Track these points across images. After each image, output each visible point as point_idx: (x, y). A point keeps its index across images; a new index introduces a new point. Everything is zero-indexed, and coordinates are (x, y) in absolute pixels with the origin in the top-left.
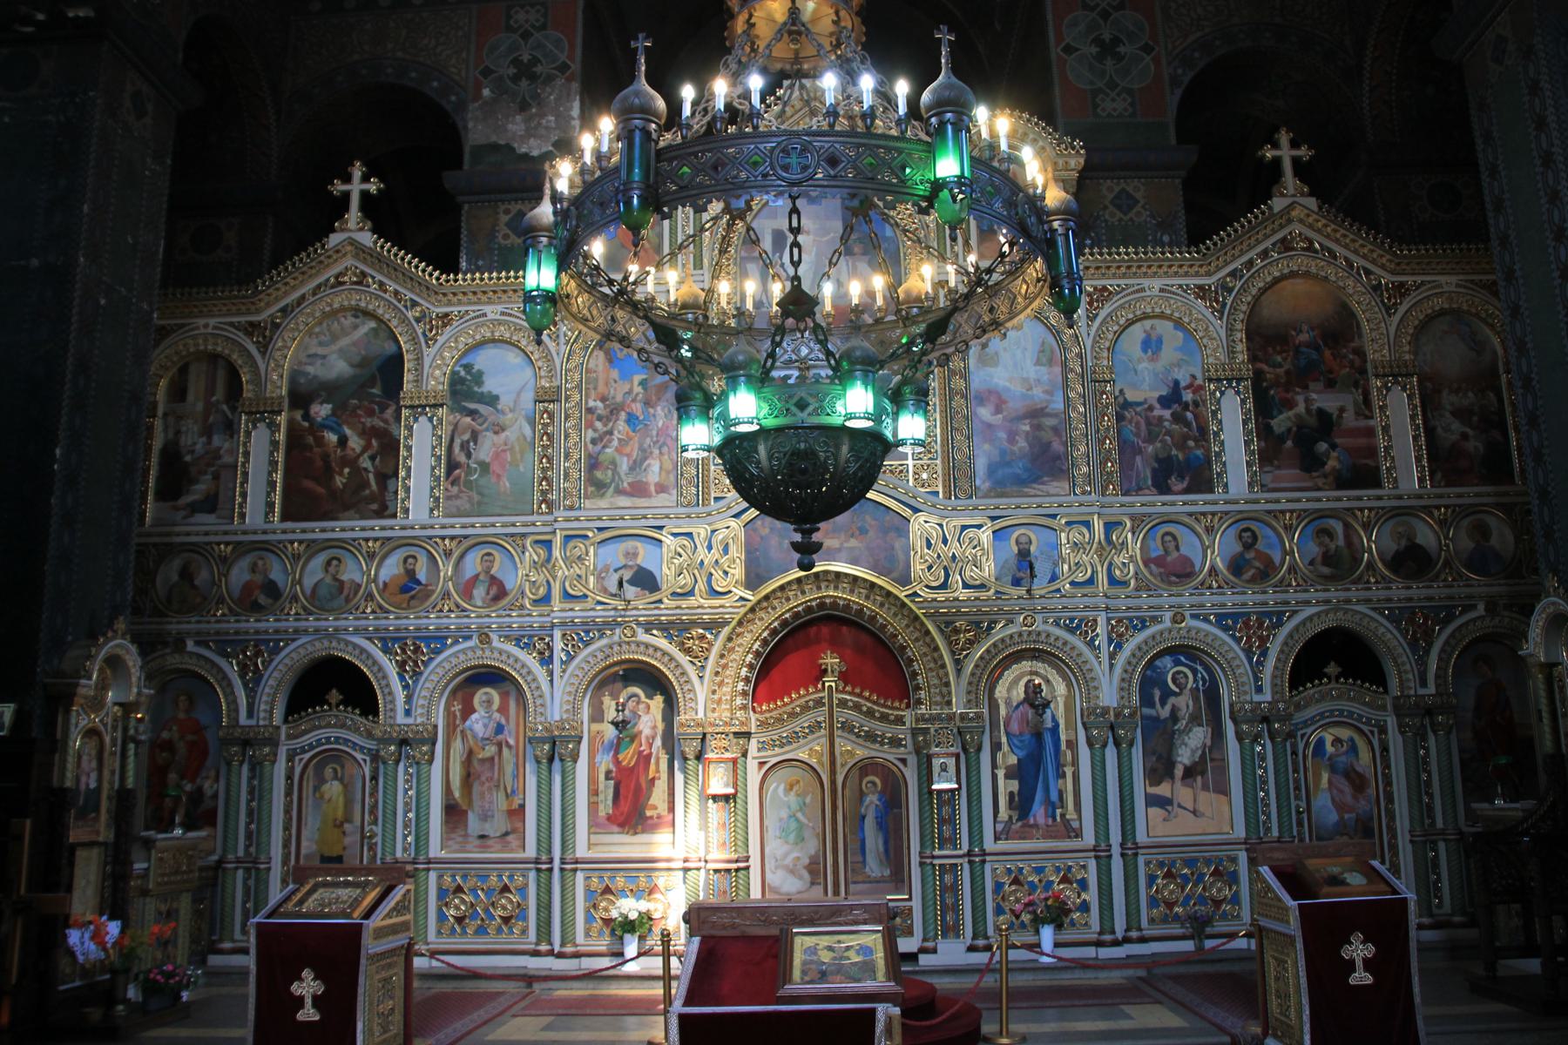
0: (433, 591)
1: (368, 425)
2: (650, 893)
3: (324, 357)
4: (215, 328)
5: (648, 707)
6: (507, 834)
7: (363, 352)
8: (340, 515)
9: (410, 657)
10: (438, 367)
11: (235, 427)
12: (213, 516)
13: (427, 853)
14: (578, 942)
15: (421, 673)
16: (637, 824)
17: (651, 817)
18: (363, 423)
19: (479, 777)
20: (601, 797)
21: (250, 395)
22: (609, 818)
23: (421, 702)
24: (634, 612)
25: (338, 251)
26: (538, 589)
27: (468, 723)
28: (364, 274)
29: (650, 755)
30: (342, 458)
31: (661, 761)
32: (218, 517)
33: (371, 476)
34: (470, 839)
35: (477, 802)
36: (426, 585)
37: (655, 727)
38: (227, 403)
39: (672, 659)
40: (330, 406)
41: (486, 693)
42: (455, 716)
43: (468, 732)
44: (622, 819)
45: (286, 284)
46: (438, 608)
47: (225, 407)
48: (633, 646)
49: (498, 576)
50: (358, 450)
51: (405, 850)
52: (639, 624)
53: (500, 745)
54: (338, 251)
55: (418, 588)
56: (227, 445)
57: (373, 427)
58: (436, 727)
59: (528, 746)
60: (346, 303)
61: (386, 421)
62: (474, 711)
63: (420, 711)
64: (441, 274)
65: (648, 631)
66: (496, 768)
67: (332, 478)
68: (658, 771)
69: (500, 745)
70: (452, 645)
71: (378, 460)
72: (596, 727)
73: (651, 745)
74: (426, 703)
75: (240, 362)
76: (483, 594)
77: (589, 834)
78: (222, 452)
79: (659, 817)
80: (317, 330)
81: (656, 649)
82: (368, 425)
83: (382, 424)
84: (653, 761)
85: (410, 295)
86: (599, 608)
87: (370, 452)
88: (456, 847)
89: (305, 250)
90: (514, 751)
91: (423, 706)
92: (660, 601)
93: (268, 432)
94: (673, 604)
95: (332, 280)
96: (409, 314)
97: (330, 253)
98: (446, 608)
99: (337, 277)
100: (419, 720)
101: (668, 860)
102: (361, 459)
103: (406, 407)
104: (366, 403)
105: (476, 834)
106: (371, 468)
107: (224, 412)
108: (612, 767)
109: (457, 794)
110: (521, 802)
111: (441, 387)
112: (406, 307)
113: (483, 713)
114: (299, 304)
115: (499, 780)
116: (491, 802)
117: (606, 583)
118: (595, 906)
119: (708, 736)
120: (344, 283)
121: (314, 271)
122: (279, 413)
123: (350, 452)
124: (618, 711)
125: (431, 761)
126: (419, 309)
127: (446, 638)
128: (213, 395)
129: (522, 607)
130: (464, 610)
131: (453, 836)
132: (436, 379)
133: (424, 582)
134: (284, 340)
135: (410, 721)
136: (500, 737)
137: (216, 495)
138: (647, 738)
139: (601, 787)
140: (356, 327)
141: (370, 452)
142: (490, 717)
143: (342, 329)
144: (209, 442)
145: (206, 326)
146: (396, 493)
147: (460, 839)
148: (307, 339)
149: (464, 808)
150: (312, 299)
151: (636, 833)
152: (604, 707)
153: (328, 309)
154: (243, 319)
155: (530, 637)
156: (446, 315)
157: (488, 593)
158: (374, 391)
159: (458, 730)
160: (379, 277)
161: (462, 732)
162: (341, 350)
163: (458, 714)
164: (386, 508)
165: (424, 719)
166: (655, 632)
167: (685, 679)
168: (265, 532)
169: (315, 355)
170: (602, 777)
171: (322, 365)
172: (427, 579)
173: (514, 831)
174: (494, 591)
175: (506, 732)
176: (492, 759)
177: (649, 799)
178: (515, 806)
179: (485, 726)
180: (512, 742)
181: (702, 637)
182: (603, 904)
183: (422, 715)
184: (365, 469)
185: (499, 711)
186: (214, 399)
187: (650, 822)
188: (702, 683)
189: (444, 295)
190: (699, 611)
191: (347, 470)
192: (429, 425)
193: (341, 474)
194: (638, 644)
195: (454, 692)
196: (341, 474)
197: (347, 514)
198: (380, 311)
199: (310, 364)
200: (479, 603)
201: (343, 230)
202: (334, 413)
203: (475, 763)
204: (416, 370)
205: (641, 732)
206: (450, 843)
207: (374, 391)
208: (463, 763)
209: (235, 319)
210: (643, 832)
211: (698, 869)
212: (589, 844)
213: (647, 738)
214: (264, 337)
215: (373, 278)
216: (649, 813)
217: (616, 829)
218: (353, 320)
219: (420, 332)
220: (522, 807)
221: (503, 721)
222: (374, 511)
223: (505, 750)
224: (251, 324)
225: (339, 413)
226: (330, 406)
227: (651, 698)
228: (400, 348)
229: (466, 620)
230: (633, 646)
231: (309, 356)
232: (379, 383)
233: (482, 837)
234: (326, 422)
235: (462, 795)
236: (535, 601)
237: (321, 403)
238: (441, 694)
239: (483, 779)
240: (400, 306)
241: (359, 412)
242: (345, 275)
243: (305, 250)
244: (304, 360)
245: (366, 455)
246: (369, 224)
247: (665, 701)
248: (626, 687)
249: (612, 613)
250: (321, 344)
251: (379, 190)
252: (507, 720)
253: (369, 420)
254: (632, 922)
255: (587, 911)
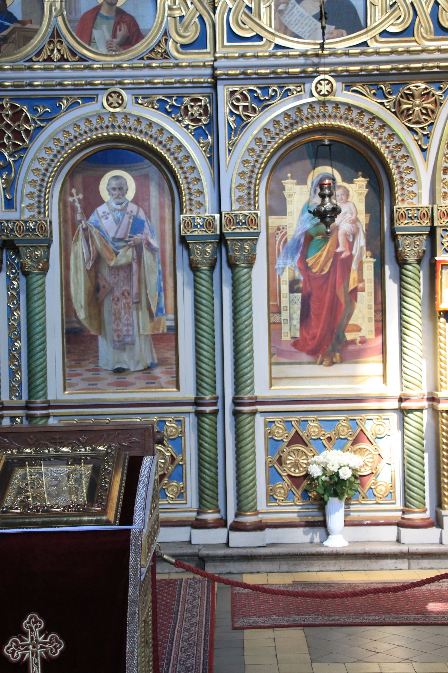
0: (36, 31)
2: (355, 442)
5: (347, 193)
6: (149, 368)
9: (8, 126)
13: (45, 394)
14: (259, 508)
15: (25, 149)
16: (334, 351)
17: (353, 342)
19: (112, 291)
20: (285, 315)
22: (296, 343)
23: (28, 189)
24: (332, 59)
26: (186, 29)
27: (92, 218)
29: (351, 257)
31: (365, 266)
34: (103, 375)
35: (109, 327)
36: (23, 23)
37: (356, 221)
39: (384, 125)
41: (116, 177)
42: (74, 209)
43: (94, 231)
44: (312, 344)
46: (44, 55)
48: (330, 108)
49: (129, 10)
51: (12, 390)
52: (338, 76)
53: (138, 248)
55: (12, 26)
58: (51, 222)
59: (179, 249)
62: (102, 202)
63: (27, 201)
65: (348, 87)
66: (135, 279)
68: (361, 280)
69: (138, 248)
70: (68, 108)
72: (274, 221)
73: (351, 246)
74: (35, 190)
76: (108, 36)
77: (271, 364)
79: (363, 341)
81: (362, 111)
84: (354, 266)
86: (279, 53)
88: (84, 385)
90: (158, 255)
91: (31, 195)
92: (365, 44)
94: (385, 47)
98: (56, 56)
100: (27, 215)
101: (380, 399)
105: (110, 368)
108: (298, 274)
109: (82, 315)
110: (172, 324)
113: (114, 205)
115: (139, 294)
116: (131, 325)
117: (286, 20)
118: (280, 461)
119: (439, 231)
124: (323, 196)
125: (44, 271)
127: (60, 99)
129: (166, 55)
130: (83, 59)
131: (79, 371)
133: (19, 17)
135: (13, 215)
136: (138, 237)
138: (346, 235)
139: (285, 302)
142: (123, 210)
147: (89, 375)
149: (93, 332)
151: (332, 363)
152: (286, 193)
155: (180, 98)
157: (114, 36)
159: (80, 227)
161: (85, 230)
163: (78, 205)
165: (35, 213)
166: (358, 88)
167: (403, 152)
170: (285, 288)
172: (24, 13)
173: (162, 362)
174: (120, 34)
175: (147, 230)
176: (129, 265)
177: (349, 318)
178: (163, 329)
179: (118, 222)
180: (155, 243)
181: (427, 95)
182: (291, 459)
183: (30, 207)
185: (135, 201)
187: (351, 348)
188: (426, 159)
190: (424, 56)
194: (337, 105)
195: (71, 174)
200: (103, 50)
203: (105, 272)
205: (337, 228)
206: (74, 380)
208: (88, 272)
210: (342, 361)
211: (421, 410)
212: (271, 378)
213: (346, 235)
216: (349, 336)
217: (305, 357)
220: (174, 330)
221: (142, 215)
223: (146, 255)
227: (351, 181)
229: (87, 73)
230: (330, 108)
233: (119, 371)
235: (89, 316)
236: (183, 46)
238: (56, 177)
239: (117, 293)
247: (369, 185)
248: (314, 168)
249: (301, 60)
252: (148, 214)
254: (341, 482)
255: (270, 467)
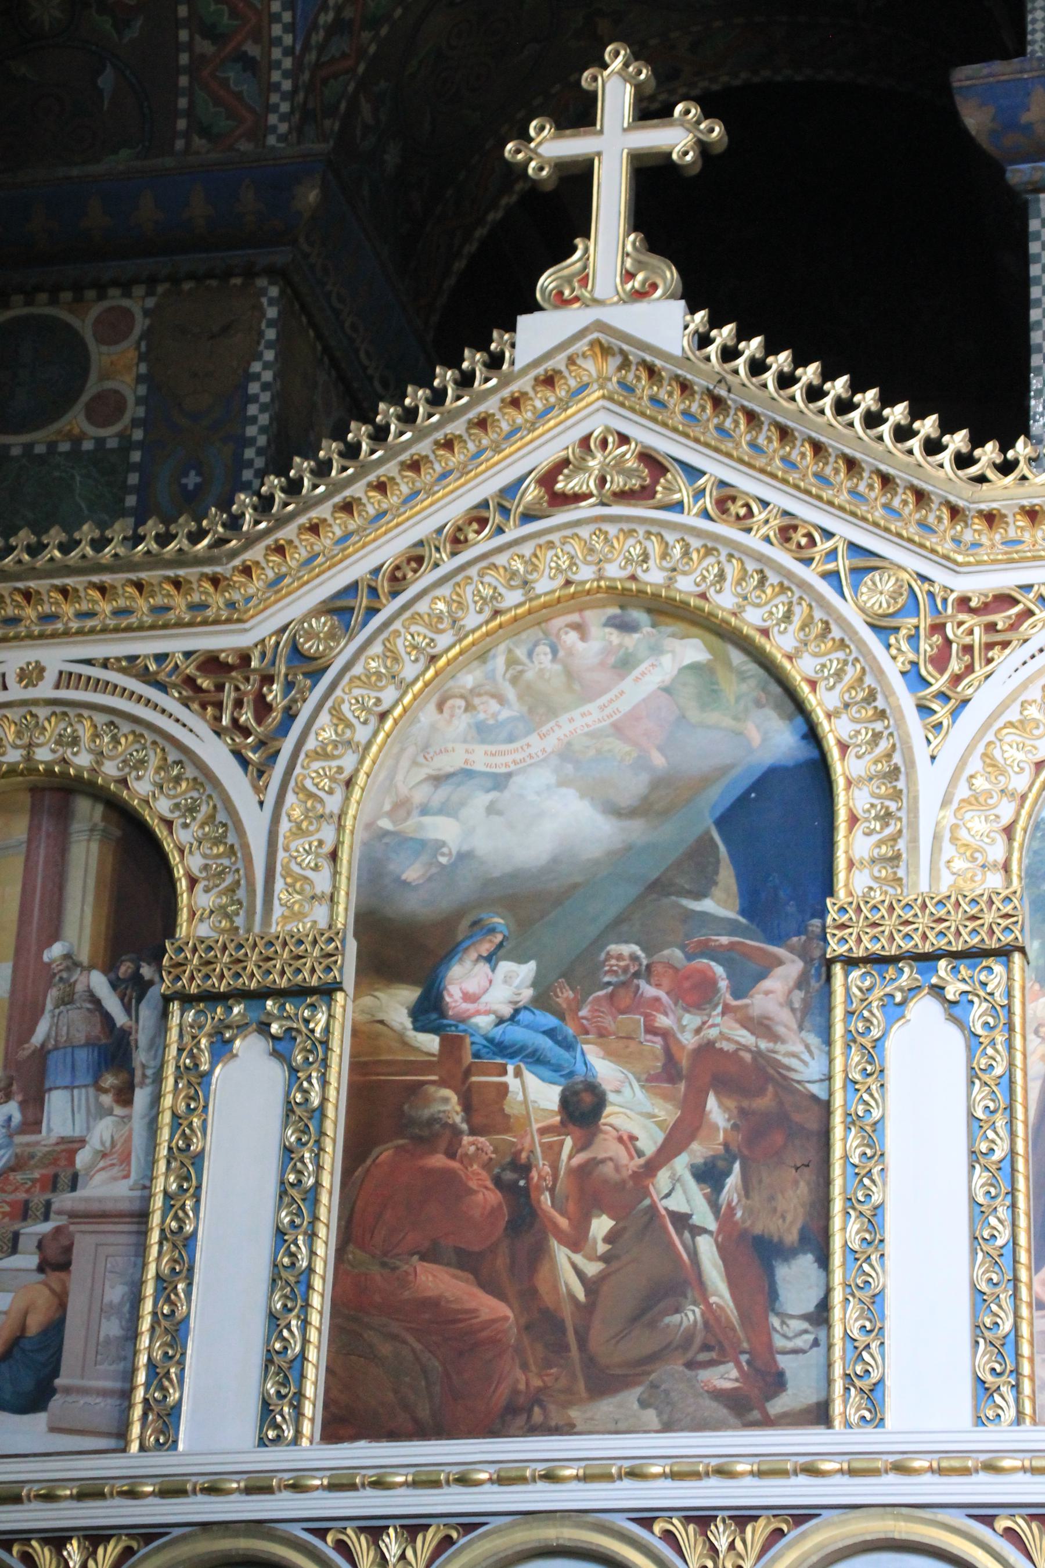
1: (689, 1040)
3: (499, 781)
4: (65, 679)
7: (658, 760)
8: (574, 1414)
10: (976, 801)
11: (141, 1057)
12: (39, 1420)
18: (665, 1034)
21: (203, 930)
25: (549, 381)
28: (652, 461)
30: (583, 1173)
32: (53, 1430)
33: (706, 1247)
38: (109, 968)
40: (528, 970)
45: (347, 507)
47: (99, 982)
50: (649, 1142)
54: (549, 381)
56: (103, 1131)
57: (707, 1050)
60: (585, 573)
61: (762, 1027)
64: (977, 441)
67: (539, 1253)
71: (733, 1180)
75: (163, 806)
78: (82, 1158)
80: (468, 680)
82: (689, 1040)
83: (745, 1037)
85: (846, 531)
87: (698, 1151)
89: (425, 380)
93: (277, 1073)
95: (532, 493)
96: (848, 610)
97: (524, 384)
99: (547, 480)
102: (663, 1178)
103: (850, 962)
104: (676, 954)
106: (704, 1217)
107: (96, 1001)
111: (995, 881)
112: (832, 577)
114: (397, 581)
120: (577, 498)
121: (456, 458)
122: (328, 991)
123: (620, 1153)
126: (887, 584)
128: (55, 936)
132: (971, 852)
134: (338, 717)
137: (55, 1329)
140: (625, 664)
141: (698, 1151)
143: (570, 674)
144: (33, 1124)
145: (31, 675)
146: (821, 1314)
148: (428, 715)
150: (449, 565)
153: (513, 597)
154: (176, 644)
156: (1005, 600)
158: (708, 905)
160: (715, 469)
162: (566, 753)
164: (777, 1382)
168: (258, 1487)
169: (467, 774)
171: (492, 809)
184: (681, 1220)
186: (56, 950)
189: (990, 518)
191: (601, 1225)
192: (954, 1039)
193: (577, 1242)
196: (577, 1242)
197: (606, 1407)
198: (724, 601)
199: (444, 810)
201: (561, 302)
202: (543, 999)
204: (886, 817)
207: (708, 905)
209: (145, 647)
214: (263, 708)
215: (693, 473)
218: (615, 637)
219: (892, 671)
222: (718, 1395)
224: (212, 663)
225: (565, 995)
226: (528, 970)
228: (812, 735)
231: (438, 780)
232: (727, 875)
234: (516, 1034)
237: (491, 959)
240: (809, 575)
241: (649, 990)
242: (581, 468)
243: (425, 380)
244: (419, 796)
245: (681, 1163)
246: (670, 275)
250: (483, 732)
251: (703, 147)
253: (692, 1021)
